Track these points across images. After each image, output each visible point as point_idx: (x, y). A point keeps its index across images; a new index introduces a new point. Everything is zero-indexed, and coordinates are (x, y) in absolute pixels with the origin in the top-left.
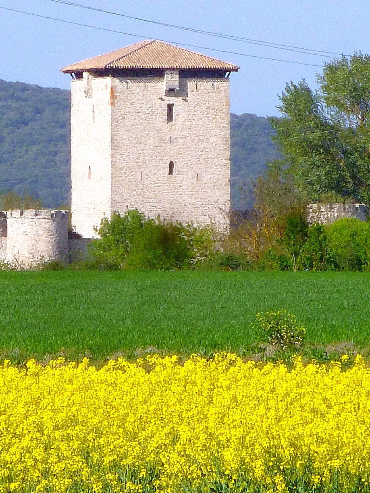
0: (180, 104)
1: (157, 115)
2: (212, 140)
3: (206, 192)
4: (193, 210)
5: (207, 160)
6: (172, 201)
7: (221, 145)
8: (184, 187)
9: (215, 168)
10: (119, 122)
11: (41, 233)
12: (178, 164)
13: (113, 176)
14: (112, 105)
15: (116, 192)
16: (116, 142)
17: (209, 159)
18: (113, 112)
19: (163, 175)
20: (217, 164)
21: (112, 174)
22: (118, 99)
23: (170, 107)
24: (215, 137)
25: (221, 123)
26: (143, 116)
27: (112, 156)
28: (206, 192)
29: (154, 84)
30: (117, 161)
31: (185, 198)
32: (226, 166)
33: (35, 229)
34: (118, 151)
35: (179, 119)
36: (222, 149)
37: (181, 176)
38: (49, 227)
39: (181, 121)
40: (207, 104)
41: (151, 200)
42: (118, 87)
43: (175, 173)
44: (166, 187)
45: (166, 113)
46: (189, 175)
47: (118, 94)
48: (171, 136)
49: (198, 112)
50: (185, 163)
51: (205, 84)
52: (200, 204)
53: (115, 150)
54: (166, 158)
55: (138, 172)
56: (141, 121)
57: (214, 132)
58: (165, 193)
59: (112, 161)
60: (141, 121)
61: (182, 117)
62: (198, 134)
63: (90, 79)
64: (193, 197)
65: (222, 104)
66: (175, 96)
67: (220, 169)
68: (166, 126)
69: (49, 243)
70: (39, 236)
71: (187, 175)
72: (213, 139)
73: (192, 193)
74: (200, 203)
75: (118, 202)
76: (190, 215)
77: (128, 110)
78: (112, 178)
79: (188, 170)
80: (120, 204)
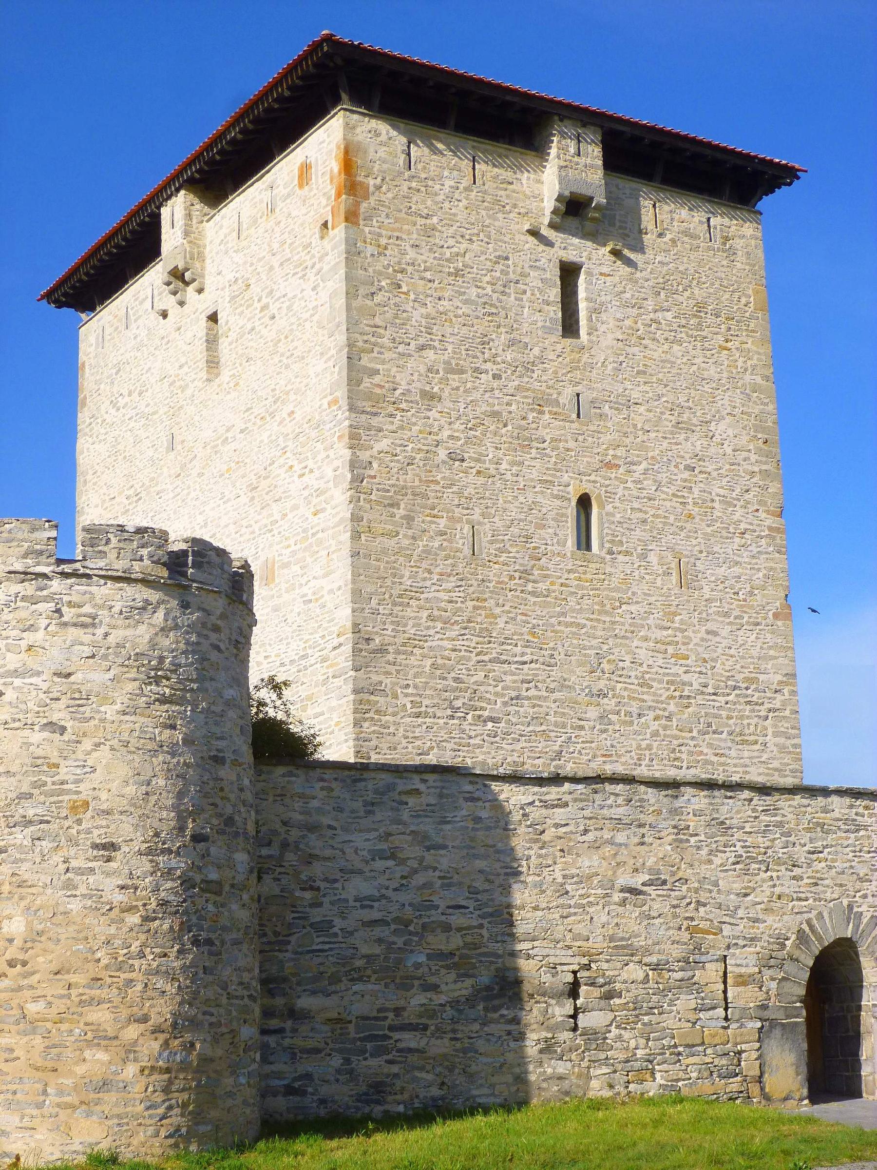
0: (605, 270)
1: (525, 297)
2: (720, 428)
3: (715, 633)
4: (672, 707)
5: (707, 504)
6: (594, 660)
7: (753, 457)
8: (633, 608)
9: (737, 540)
10: (378, 298)
11: (92, 677)
12: (609, 508)
13: (359, 526)
14: (347, 219)
15: (374, 602)
16: (366, 383)
17: (716, 505)
18: (352, 253)
19: (557, 548)
20: (743, 526)
21: (356, 518)
22: (372, 200)
23: (569, 273)
24: (729, 419)
25: (746, 370)
26: (473, 292)
27: (355, 440)
28: (715, 633)
29: (507, 174)
30: (375, 465)
31: (642, 654)
32: (774, 538)
33: (54, 657)
34: (375, 421)
35: (603, 328)
36: (756, 469)
37: (621, 558)
38: (153, 645)
39: (610, 336)
40: (696, 291)
41: (518, 650)
42: (371, 155)
43: (602, 546)
44: (572, 601)
45: (555, 293)
46: (653, 558)
47: (371, 182)
48: (578, 389)
49: (669, 315)
50: (636, 505)
51: (684, 213)
52: (696, 686)
53: (364, 416)
54: (566, 478)
55: (460, 520)
56: (465, 309)
57: (726, 402)
58: (568, 625)
59: (353, 465)
60: (465, 309)
61: (612, 323)
62: (671, 397)
63: (195, 221)
64: (671, 650)
65: (744, 300)
66: (585, 236)
67: (754, 548)
68: (559, 347)
69: (154, 753)
70: (80, 700)
71: (643, 557)
72: (722, 426)
73: (665, 633)
74: (696, 681)
75: (382, 651)
76: (665, 728)
77: (411, 254)
78: (356, 535)
79: (646, 536)
80: (390, 657)
